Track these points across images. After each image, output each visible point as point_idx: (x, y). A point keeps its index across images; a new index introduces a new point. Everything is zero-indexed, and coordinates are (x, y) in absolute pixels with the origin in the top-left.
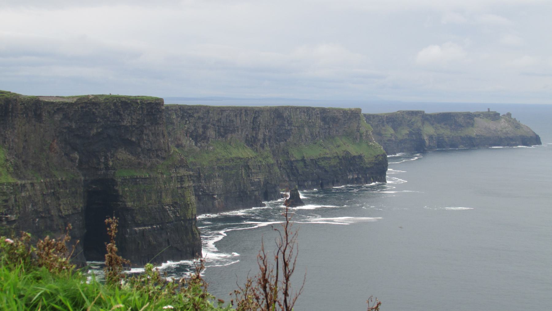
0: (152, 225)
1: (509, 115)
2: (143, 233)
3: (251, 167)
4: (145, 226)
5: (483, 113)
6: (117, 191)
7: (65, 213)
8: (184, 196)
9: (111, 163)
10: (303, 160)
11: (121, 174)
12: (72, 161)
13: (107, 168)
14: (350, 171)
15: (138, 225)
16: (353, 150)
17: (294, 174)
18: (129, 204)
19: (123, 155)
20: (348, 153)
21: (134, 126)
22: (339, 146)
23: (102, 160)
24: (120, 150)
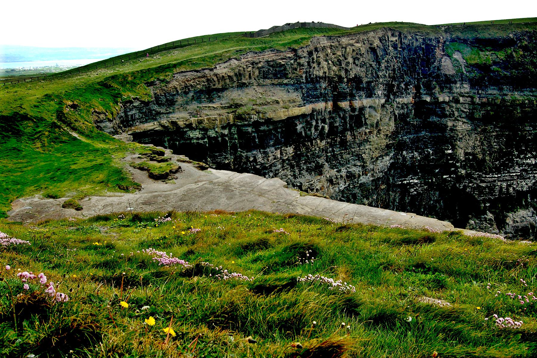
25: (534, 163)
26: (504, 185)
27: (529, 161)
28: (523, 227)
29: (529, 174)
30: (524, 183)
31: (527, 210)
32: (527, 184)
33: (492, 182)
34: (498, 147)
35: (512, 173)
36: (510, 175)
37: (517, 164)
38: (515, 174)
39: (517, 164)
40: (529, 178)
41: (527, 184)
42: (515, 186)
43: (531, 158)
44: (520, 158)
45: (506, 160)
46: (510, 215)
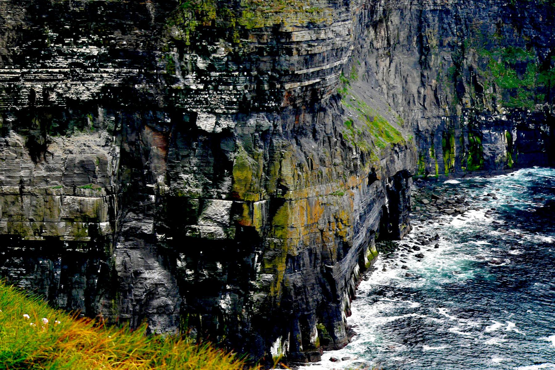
26: (39, 87)
27: (83, 50)
28: (82, 162)
29: (89, 72)
30: (81, 88)
31: (97, 135)
32: (88, 90)
33: (11, 80)
34: (13, 23)
35: (51, 67)
36: (47, 72)
37: (60, 53)
38: (57, 70)
39: (60, 53)
40: (92, 79)
41: (88, 90)
42: (60, 91)
43: (91, 44)
44: (64, 44)
45: (33, 45)
46: (58, 139)
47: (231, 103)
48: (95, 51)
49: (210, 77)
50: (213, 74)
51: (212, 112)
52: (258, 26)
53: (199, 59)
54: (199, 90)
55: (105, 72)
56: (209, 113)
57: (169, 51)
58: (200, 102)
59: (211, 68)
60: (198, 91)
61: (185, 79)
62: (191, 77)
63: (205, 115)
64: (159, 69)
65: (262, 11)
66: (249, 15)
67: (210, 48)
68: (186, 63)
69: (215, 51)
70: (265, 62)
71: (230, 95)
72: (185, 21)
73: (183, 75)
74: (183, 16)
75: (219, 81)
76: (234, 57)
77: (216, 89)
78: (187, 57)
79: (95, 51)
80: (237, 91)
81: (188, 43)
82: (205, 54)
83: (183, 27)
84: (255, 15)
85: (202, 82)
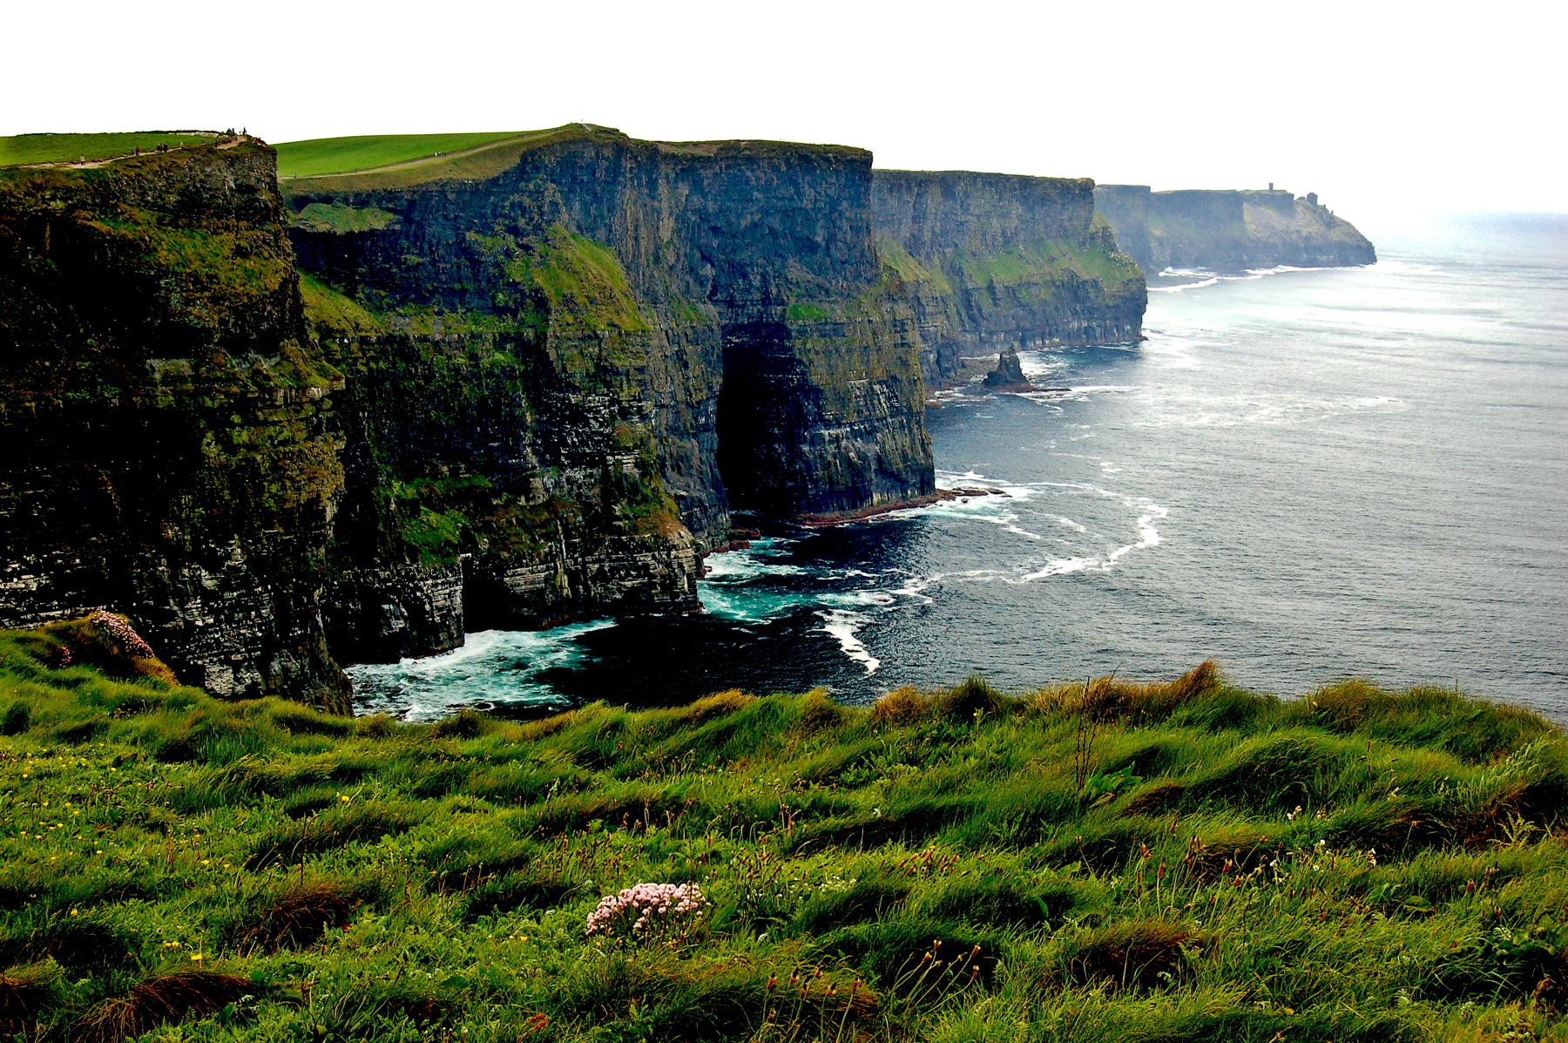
0: (851, 425)
1: (1312, 197)
2: (837, 439)
3: (923, 302)
4: (840, 425)
5: (1258, 193)
6: (790, 349)
7: (696, 397)
8: (905, 364)
9: (774, 291)
10: (991, 288)
11: (800, 313)
12: (701, 284)
13: (766, 301)
14: (1075, 314)
15: (828, 425)
16: (1085, 268)
17: (972, 319)
18: (814, 379)
19: (796, 271)
20: (1073, 275)
21: (820, 209)
22: (1053, 260)
23: (757, 282)
24: (791, 261)
25: (34, 587)
47: (255, 639)
48: (31, 583)
49: (224, 601)
50: (227, 595)
51: (228, 661)
52: (288, 506)
53: (204, 573)
54: (207, 626)
55: (49, 618)
56: (221, 663)
57: (155, 566)
58: (208, 647)
59: (225, 586)
60: (205, 629)
61: (184, 611)
62: (195, 605)
63: (216, 668)
64: (140, 599)
65: (292, 479)
66: (274, 488)
67: (220, 552)
68: (184, 583)
69: (228, 556)
70: (287, 564)
71: (251, 627)
72: (181, 510)
73: (181, 605)
74: (179, 504)
75: (237, 606)
76: (253, 561)
77: (229, 620)
78: (186, 572)
79: (31, 583)
80: (262, 618)
81: (189, 548)
82: (213, 564)
83: (178, 521)
84: (284, 487)
85: (212, 611)
